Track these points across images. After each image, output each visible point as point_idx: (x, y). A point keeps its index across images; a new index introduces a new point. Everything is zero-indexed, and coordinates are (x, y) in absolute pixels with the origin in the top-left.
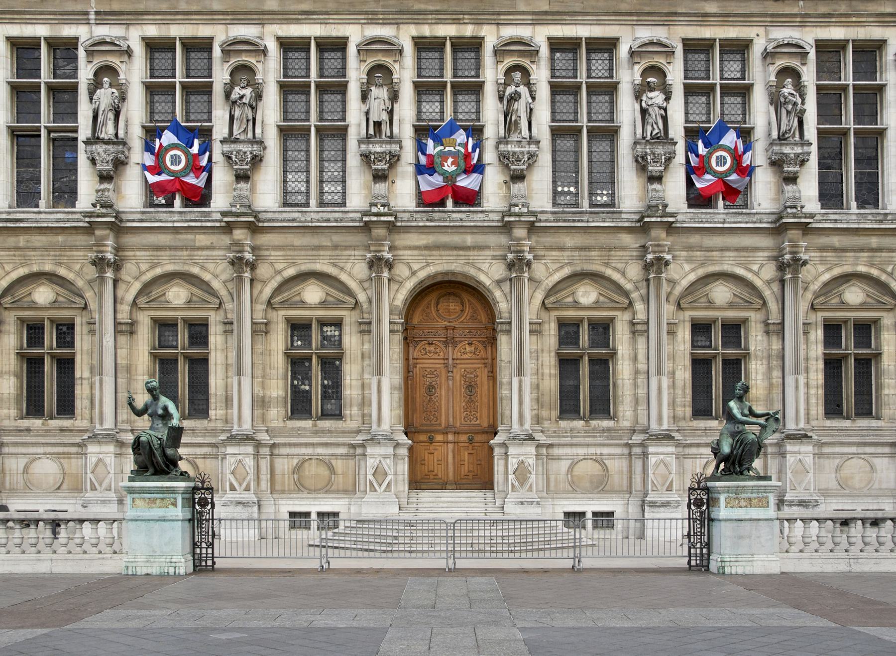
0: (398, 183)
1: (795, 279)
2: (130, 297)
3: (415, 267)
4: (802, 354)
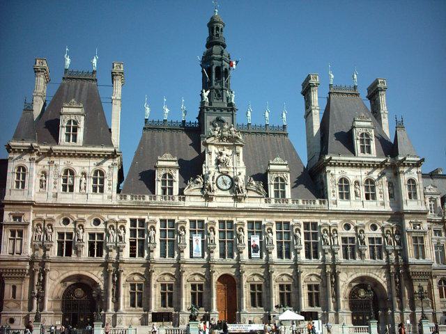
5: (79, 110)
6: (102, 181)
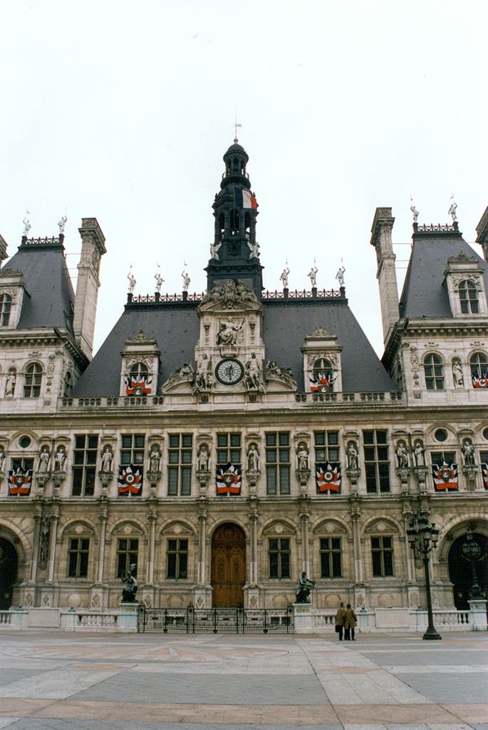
0: (210, 487)
1: (356, 522)
2: (111, 530)
3: (216, 519)
4: (360, 551)
5: (17, 280)
6: (39, 377)
